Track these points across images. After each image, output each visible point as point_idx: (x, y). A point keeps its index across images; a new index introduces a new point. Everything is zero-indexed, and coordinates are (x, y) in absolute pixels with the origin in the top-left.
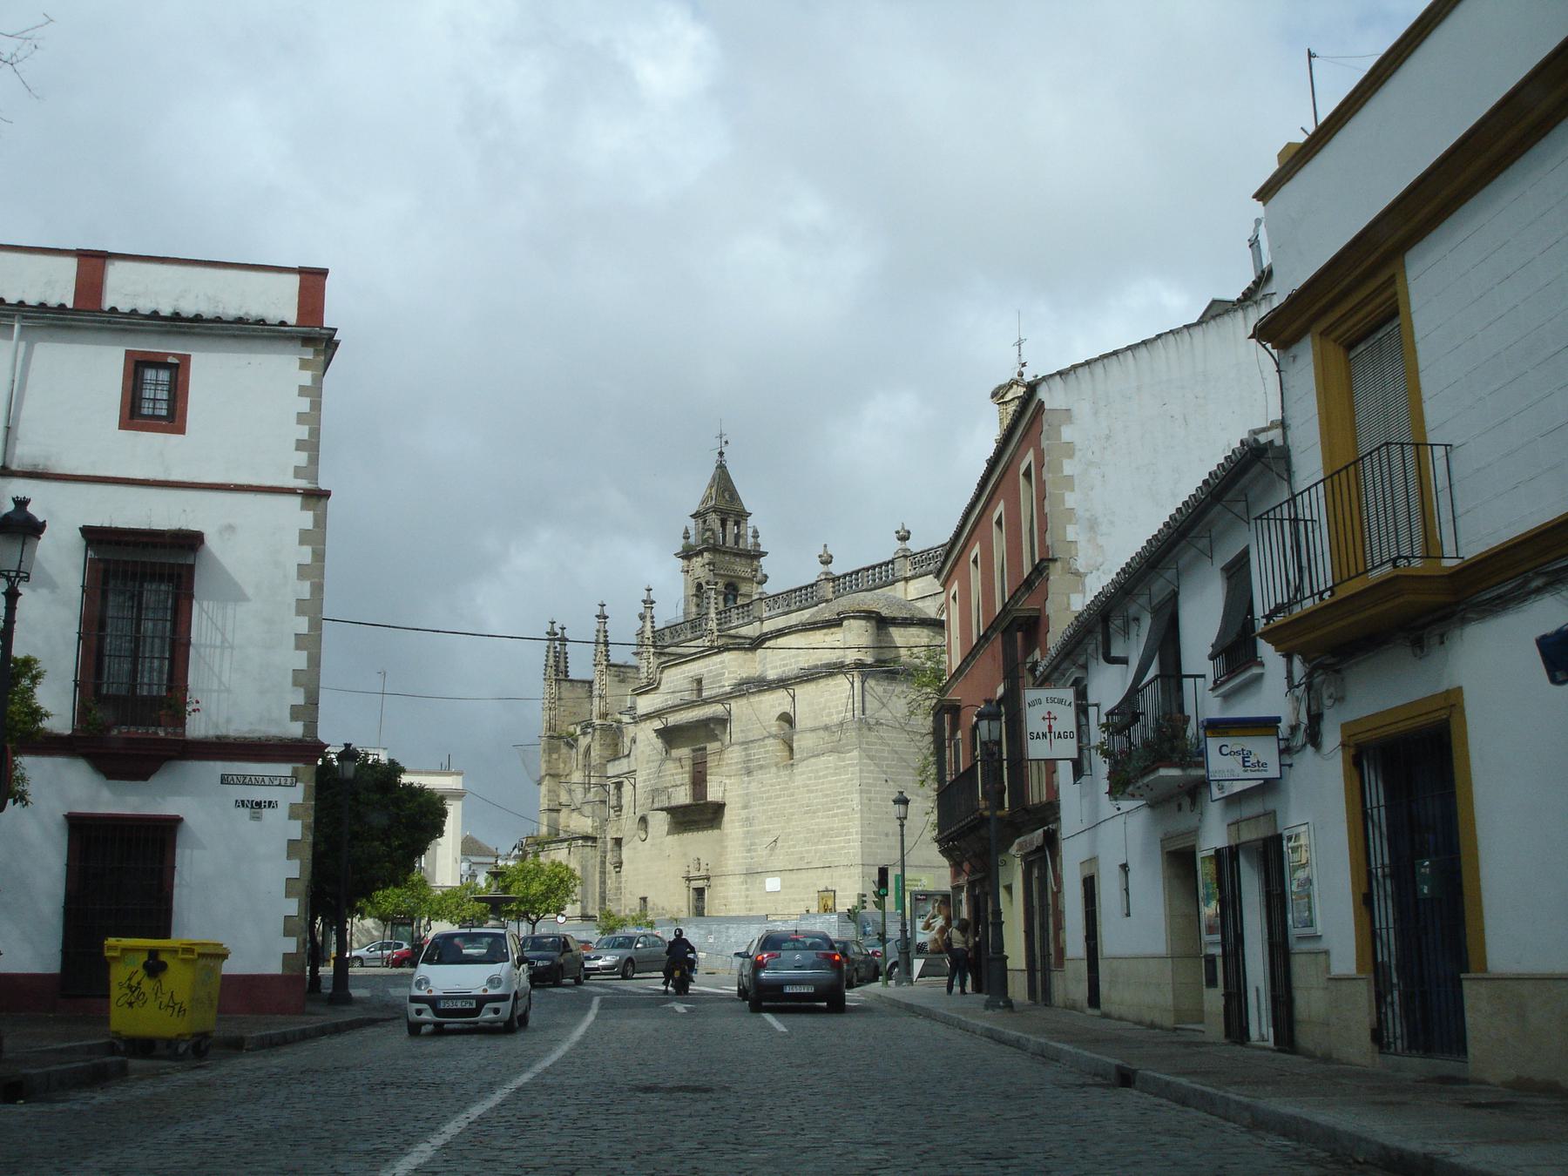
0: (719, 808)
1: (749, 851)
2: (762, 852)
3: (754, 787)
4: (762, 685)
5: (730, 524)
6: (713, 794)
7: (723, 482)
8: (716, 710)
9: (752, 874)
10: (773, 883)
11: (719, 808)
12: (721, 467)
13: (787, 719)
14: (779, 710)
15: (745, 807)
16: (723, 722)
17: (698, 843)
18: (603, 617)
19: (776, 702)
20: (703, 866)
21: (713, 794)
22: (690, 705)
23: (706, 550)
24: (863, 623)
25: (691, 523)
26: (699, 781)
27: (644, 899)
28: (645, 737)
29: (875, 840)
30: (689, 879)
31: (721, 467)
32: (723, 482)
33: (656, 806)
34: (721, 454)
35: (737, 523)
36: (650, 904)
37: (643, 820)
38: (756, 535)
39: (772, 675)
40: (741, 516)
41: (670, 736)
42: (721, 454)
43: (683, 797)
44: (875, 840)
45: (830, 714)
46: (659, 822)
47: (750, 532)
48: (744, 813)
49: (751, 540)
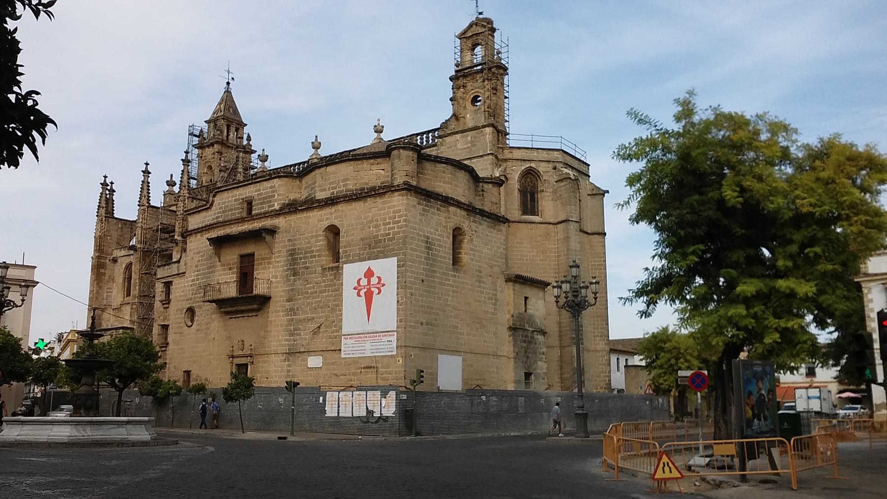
0: (264, 300)
1: (292, 335)
2: (305, 335)
3: (299, 284)
4: (311, 204)
5: (233, 129)
6: (260, 288)
7: (228, 101)
8: (268, 223)
9: (292, 353)
10: (315, 361)
11: (264, 300)
12: (228, 92)
13: (334, 231)
14: (326, 224)
15: (290, 300)
16: (272, 232)
17: (244, 329)
18: (146, 173)
19: (319, 219)
20: (247, 346)
21: (260, 288)
22: (241, 220)
23: (217, 142)
24: (410, 153)
25: (205, 127)
26: (246, 278)
27: (188, 373)
28: (199, 245)
29: (414, 327)
30: (233, 357)
31: (228, 92)
32: (228, 101)
33: (207, 299)
34: (228, 83)
35: (237, 130)
36: (193, 376)
37: (191, 311)
38: (249, 139)
39: (321, 195)
40: (241, 125)
41: (219, 243)
42: (228, 83)
43: (231, 291)
44: (414, 327)
45: (377, 226)
46: (206, 313)
47: (245, 136)
48: (288, 305)
49: (245, 142)
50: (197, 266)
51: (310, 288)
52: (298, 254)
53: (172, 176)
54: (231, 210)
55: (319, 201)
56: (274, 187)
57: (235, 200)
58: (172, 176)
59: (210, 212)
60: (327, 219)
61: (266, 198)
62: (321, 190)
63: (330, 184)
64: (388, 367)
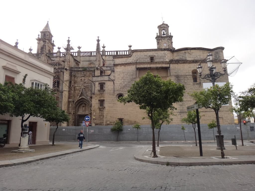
1: (182, 106)
7: (47, 26)
12: (48, 23)
14: (193, 69)
22: (148, 63)
50: (122, 78)
51: (188, 90)
52: (180, 78)
53: (31, 47)
54: (143, 59)
55: (187, 61)
56: (165, 53)
57: (145, 56)
58: (31, 47)
59: (130, 58)
60: (193, 67)
61: (162, 57)
62: (189, 57)
63: (193, 56)
64: (227, 117)
